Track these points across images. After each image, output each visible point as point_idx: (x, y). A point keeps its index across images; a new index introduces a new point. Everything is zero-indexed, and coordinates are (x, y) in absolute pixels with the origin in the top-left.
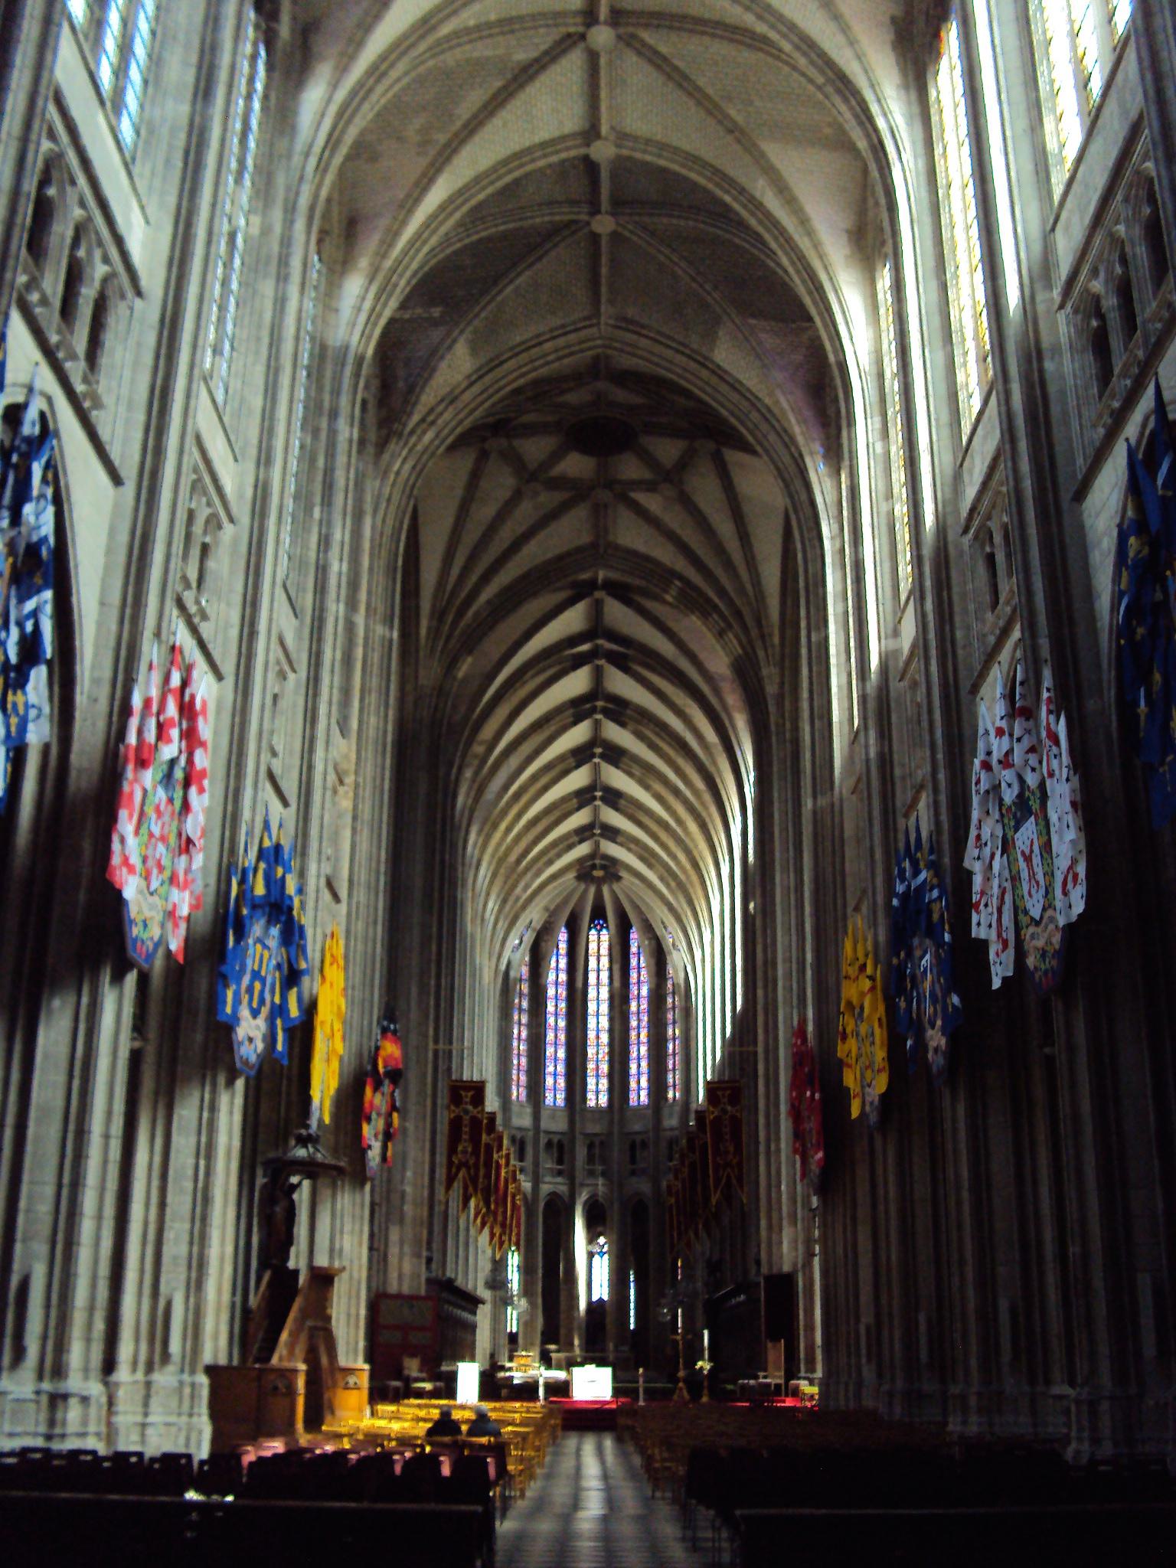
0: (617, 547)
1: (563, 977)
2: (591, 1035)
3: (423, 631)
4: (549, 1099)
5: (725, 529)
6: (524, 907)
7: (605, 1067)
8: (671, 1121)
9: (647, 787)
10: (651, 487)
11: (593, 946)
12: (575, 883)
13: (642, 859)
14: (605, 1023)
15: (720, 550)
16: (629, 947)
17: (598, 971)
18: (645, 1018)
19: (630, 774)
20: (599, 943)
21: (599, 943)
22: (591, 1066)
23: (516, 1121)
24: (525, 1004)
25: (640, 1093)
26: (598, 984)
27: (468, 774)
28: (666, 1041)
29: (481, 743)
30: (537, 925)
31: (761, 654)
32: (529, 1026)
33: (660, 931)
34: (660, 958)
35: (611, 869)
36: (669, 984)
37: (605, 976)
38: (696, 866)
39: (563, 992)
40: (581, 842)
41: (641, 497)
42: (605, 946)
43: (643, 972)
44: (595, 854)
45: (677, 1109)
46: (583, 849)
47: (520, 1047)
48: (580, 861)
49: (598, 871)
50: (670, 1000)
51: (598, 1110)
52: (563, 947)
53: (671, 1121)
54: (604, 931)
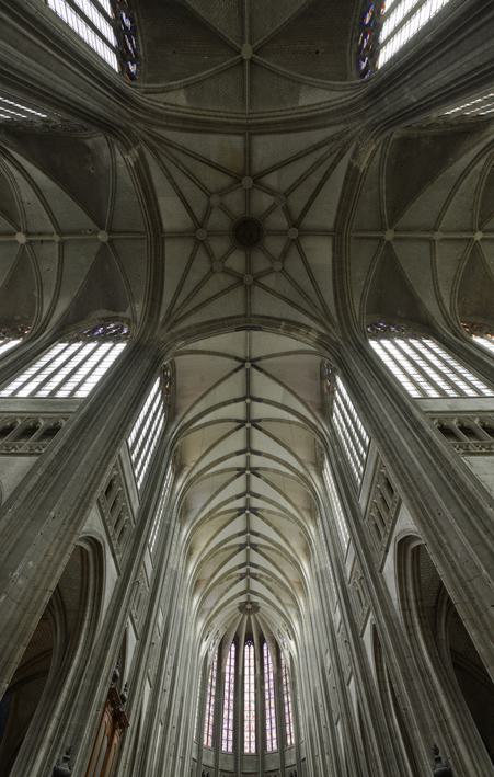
0: (255, 316)
1: (233, 670)
2: (246, 704)
3: (161, 319)
4: (224, 748)
5: (305, 282)
6: (215, 615)
7: (253, 725)
8: (291, 760)
9: (269, 524)
10: (270, 271)
11: (247, 654)
13: (268, 588)
14: (253, 698)
15: (302, 292)
18: (272, 692)
19: (262, 518)
20: (249, 652)
21: (249, 652)
22: (246, 724)
23: (204, 761)
24: (214, 684)
25: (272, 745)
27: (185, 474)
28: (284, 705)
30: (221, 635)
31: (330, 327)
32: (216, 697)
33: (277, 638)
34: (278, 652)
35: (256, 608)
37: (252, 669)
39: (232, 677)
40: (241, 579)
41: (262, 281)
42: (252, 653)
43: (271, 666)
44: (248, 591)
45: (293, 750)
46: (241, 586)
47: (210, 709)
48: (241, 594)
49: (249, 608)
51: (250, 755)
52: (233, 653)
53: (291, 760)
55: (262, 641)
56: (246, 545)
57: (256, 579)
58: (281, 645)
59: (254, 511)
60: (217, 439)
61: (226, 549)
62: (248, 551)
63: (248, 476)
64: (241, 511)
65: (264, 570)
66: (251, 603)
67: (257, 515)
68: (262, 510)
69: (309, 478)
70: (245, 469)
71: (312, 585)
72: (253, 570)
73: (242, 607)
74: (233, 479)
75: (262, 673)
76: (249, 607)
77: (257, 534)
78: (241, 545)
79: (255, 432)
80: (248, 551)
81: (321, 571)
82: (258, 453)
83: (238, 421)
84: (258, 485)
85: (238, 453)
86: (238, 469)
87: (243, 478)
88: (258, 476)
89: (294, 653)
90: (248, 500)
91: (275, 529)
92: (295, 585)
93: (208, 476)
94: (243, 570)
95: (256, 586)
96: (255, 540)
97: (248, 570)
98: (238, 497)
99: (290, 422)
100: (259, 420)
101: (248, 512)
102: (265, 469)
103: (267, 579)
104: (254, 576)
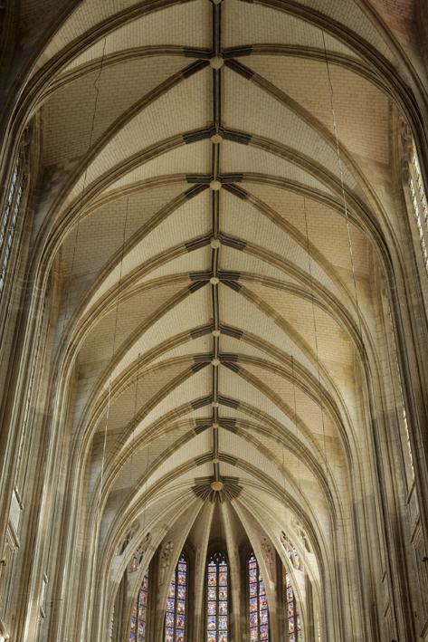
1: (181, 606)
11: (212, 577)
12: (192, 494)
13: (262, 449)
16: (248, 576)
17: (218, 601)
19: (250, 296)
24: (141, 630)
26: (217, 615)
29: (72, 160)
30: (155, 543)
36: (290, 607)
37: (223, 605)
38: (327, 400)
42: (223, 577)
44: (213, 455)
46: (200, 444)
48: (199, 461)
49: (217, 489)
50: (291, 625)
52: (182, 576)
54: (223, 563)
55: (245, 552)
56: (211, 356)
57: (234, 431)
58: (286, 562)
59: (231, 279)
60: (133, 101)
61: (162, 366)
62: (215, 371)
63: (215, 197)
64: (198, 280)
65: (256, 412)
66: (224, 479)
67: (237, 288)
68: (251, 277)
69: (371, 204)
70: (210, 178)
71: (362, 445)
72: (226, 411)
73: (202, 490)
74: (177, 203)
75: (245, 612)
76: (218, 486)
77: (237, 333)
78: (197, 357)
79: (231, 79)
80: (215, 371)
81: (384, 416)
82: (242, 137)
83: (188, 52)
84: (238, 217)
85: (190, 137)
86: (190, 178)
87: (202, 199)
88: (242, 195)
89: (315, 576)
90: (214, 255)
91: (281, 322)
92: (321, 442)
93: (114, 196)
94: (203, 412)
95: (230, 443)
96: (229, 345)
97: (215, 411)
98: (192, 245)
99: (326, 56)
100: (246, 50)
101: (214, 281)
102: (261, 178)
103: (260, 430)
104: (230, 424)
